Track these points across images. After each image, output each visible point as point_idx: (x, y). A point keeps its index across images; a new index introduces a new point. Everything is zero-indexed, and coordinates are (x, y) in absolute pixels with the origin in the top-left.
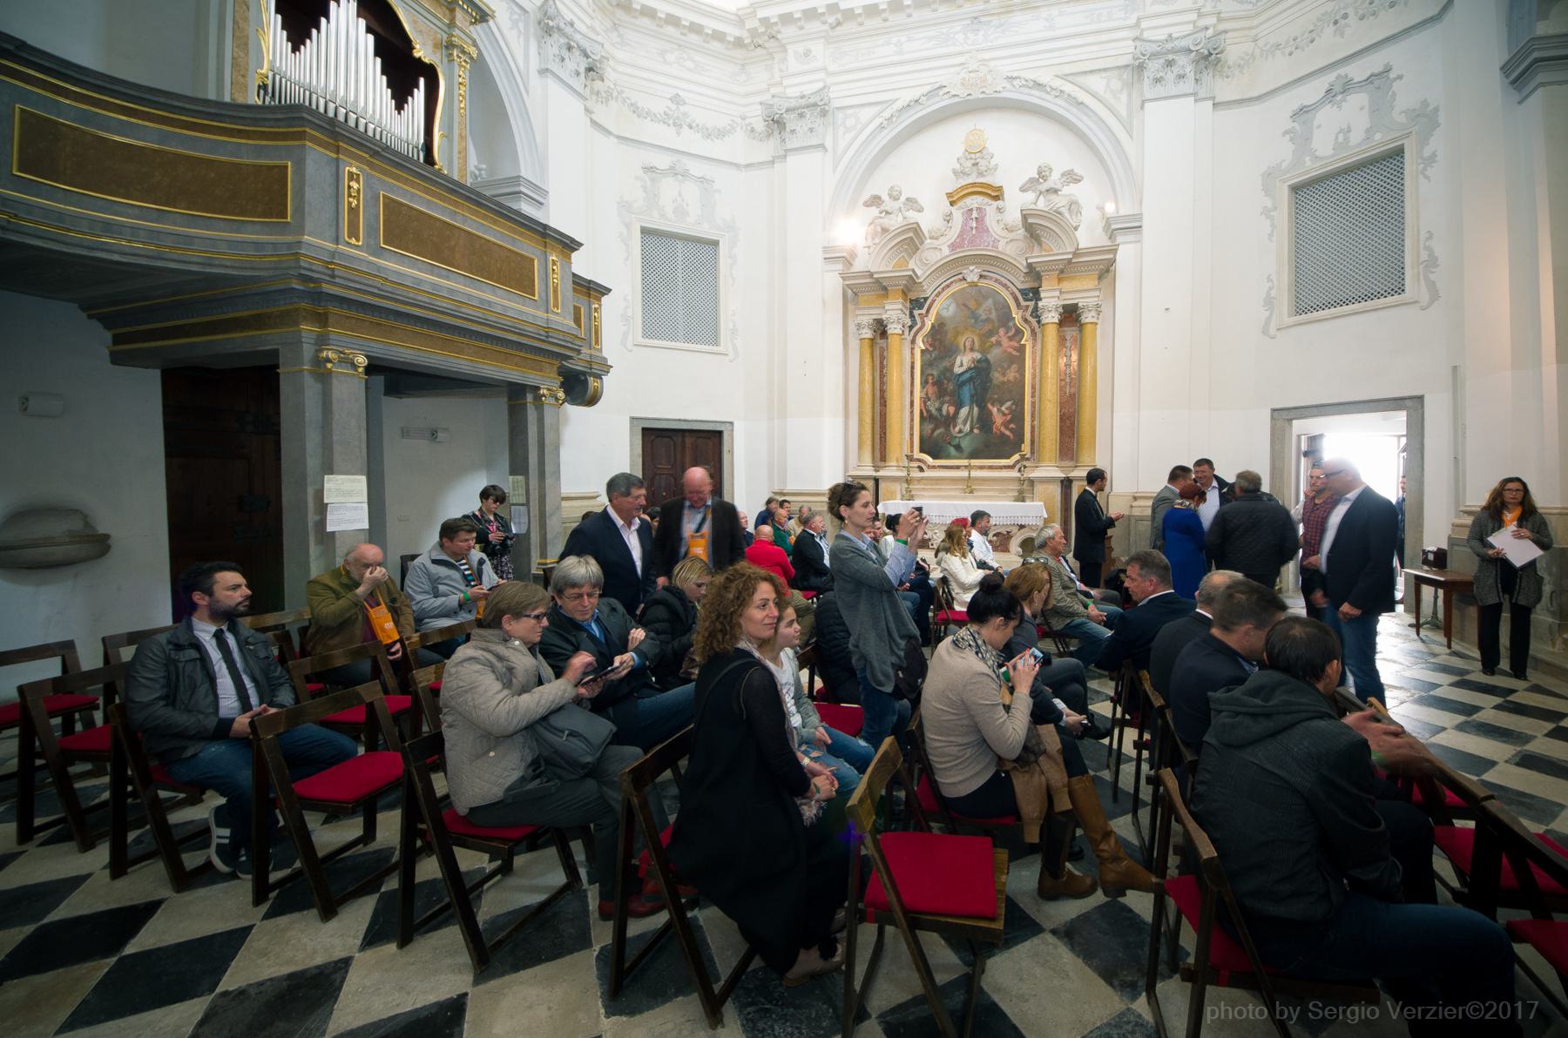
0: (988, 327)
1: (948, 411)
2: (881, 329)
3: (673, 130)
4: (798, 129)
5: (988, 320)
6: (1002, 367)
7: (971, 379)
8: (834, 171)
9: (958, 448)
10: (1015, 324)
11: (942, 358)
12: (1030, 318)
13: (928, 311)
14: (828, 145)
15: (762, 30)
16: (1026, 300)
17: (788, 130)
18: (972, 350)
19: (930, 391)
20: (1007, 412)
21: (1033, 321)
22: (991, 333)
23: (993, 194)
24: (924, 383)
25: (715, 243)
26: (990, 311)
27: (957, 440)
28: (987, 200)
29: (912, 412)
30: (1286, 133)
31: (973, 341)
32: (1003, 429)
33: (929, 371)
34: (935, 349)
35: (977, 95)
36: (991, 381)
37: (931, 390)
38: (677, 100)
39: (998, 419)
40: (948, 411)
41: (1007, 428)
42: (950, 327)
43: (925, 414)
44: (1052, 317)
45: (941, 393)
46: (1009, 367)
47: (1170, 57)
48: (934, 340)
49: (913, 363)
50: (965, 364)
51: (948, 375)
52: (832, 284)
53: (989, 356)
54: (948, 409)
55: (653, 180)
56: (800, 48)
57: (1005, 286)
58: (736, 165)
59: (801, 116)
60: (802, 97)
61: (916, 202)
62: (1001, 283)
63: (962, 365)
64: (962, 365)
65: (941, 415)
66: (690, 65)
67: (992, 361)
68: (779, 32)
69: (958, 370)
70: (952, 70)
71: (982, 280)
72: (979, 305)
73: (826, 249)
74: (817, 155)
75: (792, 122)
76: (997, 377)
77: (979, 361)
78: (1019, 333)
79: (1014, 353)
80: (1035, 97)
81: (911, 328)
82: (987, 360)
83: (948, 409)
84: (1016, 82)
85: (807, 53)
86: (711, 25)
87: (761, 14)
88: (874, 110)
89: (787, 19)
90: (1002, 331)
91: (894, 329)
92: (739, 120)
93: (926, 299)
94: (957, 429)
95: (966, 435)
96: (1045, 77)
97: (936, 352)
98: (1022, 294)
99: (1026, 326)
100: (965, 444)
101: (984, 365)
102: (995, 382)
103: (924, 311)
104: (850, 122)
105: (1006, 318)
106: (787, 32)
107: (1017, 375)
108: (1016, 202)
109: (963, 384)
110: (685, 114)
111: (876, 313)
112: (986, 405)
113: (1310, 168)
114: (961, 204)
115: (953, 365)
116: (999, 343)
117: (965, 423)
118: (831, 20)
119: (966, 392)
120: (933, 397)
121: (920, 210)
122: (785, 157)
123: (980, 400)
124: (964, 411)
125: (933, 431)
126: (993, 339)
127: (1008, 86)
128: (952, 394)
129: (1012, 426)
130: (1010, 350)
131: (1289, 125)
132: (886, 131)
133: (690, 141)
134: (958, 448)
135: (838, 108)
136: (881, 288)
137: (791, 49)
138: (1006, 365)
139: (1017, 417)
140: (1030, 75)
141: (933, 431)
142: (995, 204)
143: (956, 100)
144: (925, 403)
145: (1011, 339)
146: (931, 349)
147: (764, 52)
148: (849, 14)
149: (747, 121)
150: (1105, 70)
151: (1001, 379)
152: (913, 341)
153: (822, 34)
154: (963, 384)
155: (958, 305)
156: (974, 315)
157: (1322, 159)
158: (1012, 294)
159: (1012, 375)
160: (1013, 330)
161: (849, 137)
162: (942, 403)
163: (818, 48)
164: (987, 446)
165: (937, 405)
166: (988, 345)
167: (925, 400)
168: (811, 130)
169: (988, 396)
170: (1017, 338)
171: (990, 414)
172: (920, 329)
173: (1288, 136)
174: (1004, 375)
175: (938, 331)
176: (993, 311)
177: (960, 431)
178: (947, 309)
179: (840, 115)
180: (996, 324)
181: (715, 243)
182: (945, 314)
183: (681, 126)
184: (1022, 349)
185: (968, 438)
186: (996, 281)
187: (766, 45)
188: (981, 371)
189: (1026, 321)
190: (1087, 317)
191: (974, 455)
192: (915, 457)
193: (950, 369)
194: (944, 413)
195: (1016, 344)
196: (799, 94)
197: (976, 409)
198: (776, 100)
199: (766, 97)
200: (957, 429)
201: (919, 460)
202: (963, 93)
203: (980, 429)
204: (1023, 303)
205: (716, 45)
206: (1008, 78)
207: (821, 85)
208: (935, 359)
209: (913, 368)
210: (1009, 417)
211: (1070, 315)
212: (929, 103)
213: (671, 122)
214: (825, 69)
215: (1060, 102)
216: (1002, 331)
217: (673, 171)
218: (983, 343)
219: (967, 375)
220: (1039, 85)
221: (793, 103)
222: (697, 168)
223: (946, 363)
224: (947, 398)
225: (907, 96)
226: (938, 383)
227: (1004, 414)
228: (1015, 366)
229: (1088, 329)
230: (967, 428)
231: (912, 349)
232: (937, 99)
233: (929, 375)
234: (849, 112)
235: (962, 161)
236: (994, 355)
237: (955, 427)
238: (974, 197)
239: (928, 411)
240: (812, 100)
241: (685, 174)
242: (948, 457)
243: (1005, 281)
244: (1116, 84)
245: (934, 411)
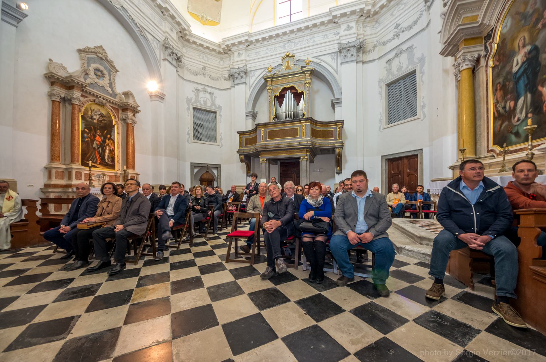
9: (517, 134)
11: (504, 67)
27: (516, 128)
31: (525, 39)
37: (499, 94)
40: (510, 107)
48: (499, 55)
49: (487, 81)
51: (509, 77)
63: (518, 63)
65: (506, 111)
67: (539, 46)
69: (515, 69)
77: (530, 52)
93: (492, 30)
94: (516, 119)
97: (501, 64)
112: (537, 89)
119: (522, 84)
120: (500, 100)
124: (521, 101)
125: (501, 126)
134: (517, 134)
141: (501, 126)
144: (496, 106)
146: (498, 64)
152: (487, 66)
154: (519, 78)
162: (506, 102)
165: (503, 104)
167: (495, 105)
172: (490, 54)
177: (519, 120)
192: (490, 149)
193: (510, 72)
194: (507, 109)
197: (529, 96)
200: (516, 119)
201: (492, 151)
208: (501, 69)
209: (487, 84)
219: (522, 69)
223: (507, 69)
224: (509, 96)
226: (504, 88)
231: (486, 71)
233: (498, 84)
239: (498, 112)
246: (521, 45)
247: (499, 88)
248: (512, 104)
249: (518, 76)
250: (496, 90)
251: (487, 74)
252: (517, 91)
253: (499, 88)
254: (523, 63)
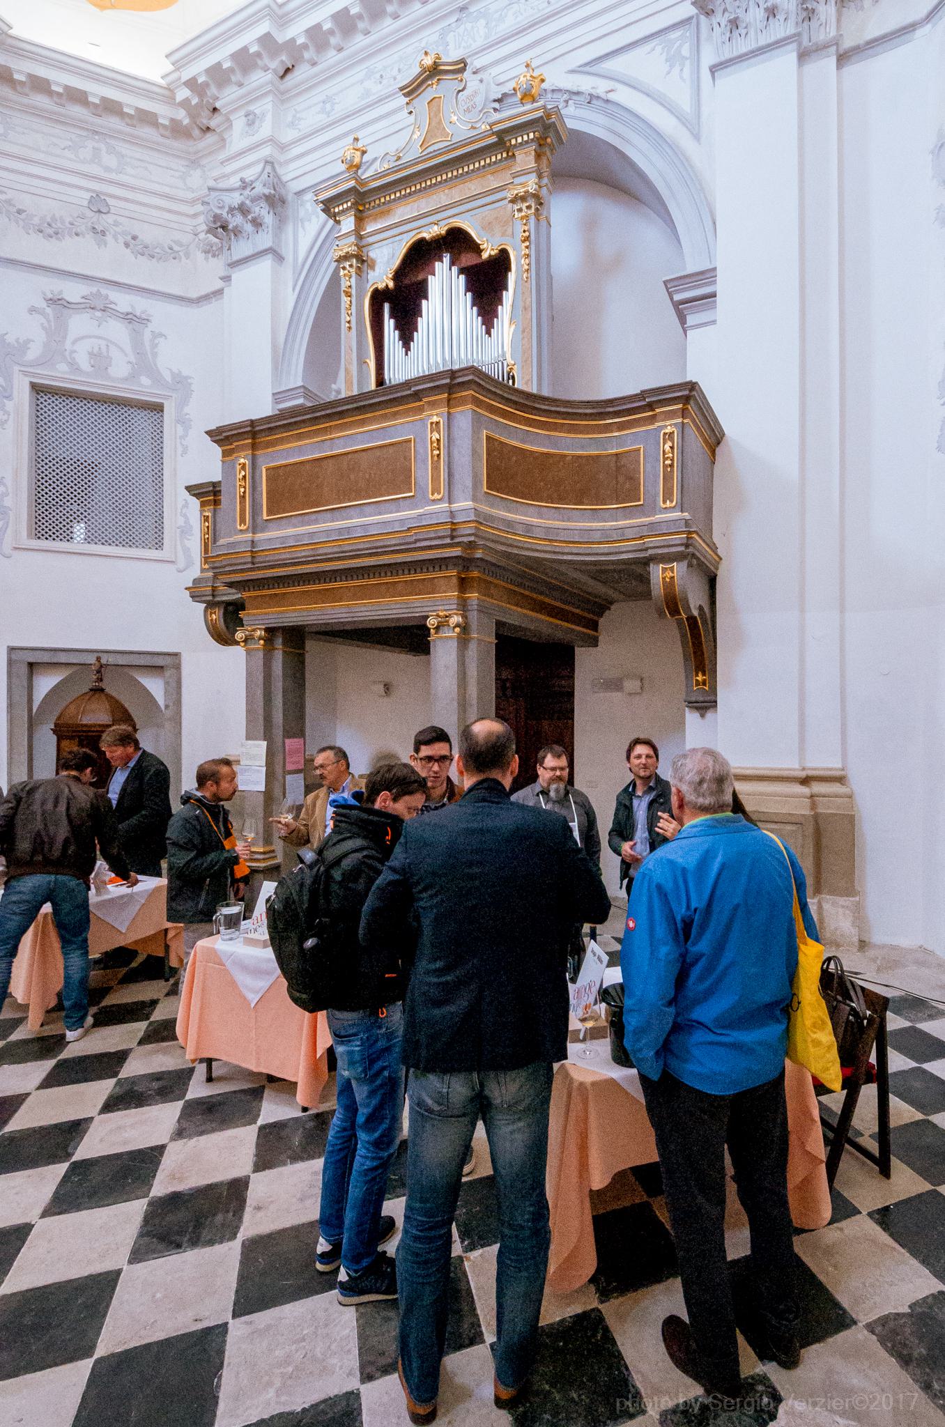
15: (195, 101)
25: (158, 408)
66: (111, 161)
74: (267, 263)
86: (131, 102)
89: (219, 75)
106: (227, 97)
118: (276, 64)
135: (299, 193)
153: (269, 88)
181: (158, 408)
187: (212, 124)
198: (214, 194)
205: (147, 132)
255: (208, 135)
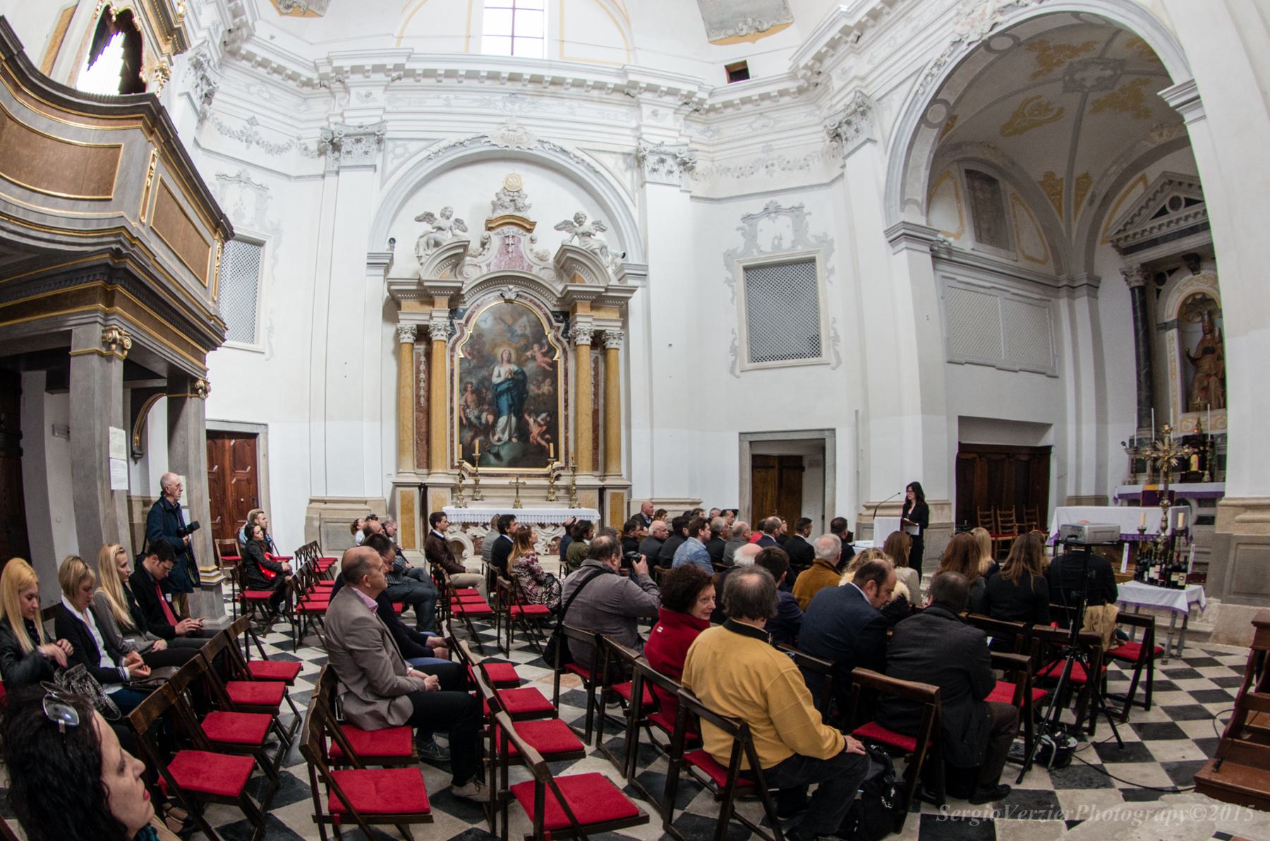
0: (522, 342)
1: (487, 421)
2: (423, 334)
3: (244, 143)
4: (354, 151)
5: (523, 336)
6: (538, 381)
7: (508, 390)
8: (381, 188)
9: (497, 456)
10: (548, 342)
11: (481, 367)
12: (561, 338)
13: (467, 321)
14: (379, 168)
16: (558, 321)
17: (343, 150)
18: (509, 361)
19: (469, 399)
20: (542, 423)
21: (564, 341)
22: (527, 347)
23: (528, 227)
24: (463, 391)
26: (525, 327)
28: (521, 231)
29: (452, 419)
30: (738, 229)
31: (510, 354)
32: (539, 439)
33: (468, 379)
34: (473, 358)
35: (513, 147)
36: (527, 393)
37: (470, 397)
38: (252, 121)
39: (535, 430)
40: (487, 421)
41: (543, 438)
42: (487, 339)
43: (464, 421)
44: (585, 340)
45: (480, 401)
46: (543, 381)
47: (664, 157)
49: (452, 370)
50: (502, 374)
51: (487, 383)
52: (375, 290)
53: (525, 369)
54: (487, 417)
55: (222, 186)
56: (363, 91)
57: (538, 306)
58: (288, 176)
59: (358, 141)
60: (361, 127)
61: (463, 223)
62: (535, 304)
63: (499, 376)
64: (499, 376)
65: (480, 423)
67: (527, 374)
68: (348, 78)
69: (496, 380)
70: (495, 126)
71: (518, 299)
72: (515, 320)
73: (370, 255)
74: (370, 173)
75: (347, 145)
76: (532, 389)
77: (516, 373)
78: (551, 350)
79: (548, 368)
80: (560, 159)
81: (450, 335)
82: (523, 373)
83: (487, 417)
84: (545, 145)
85: (368, 95)
87: (336, 64)
88: (423, 144)
90: (536, 347)
91: (437, 336)
92: (295, 140)
94: (496, 438)
95: (505, 443)
96: (569, 147)
97: (475, 361)
98: (554, 316)
99: (558, 345)
100: (504, 452)
101: (520, 377)
102: (531, 394)
103: (463, 321)
104: (399, 151)
105: (539, 336)
107: (551, 389)
108: (549, 242)
109: (501, 393)
110: (256, 133)
111: (422, 319)
112: (523, 416)
113: (756, 258)
114: (499, 230)
115: (491, 375)
116: (533, 358)
117: (503, 431)
118: (395, 75)
119: (504, 402)
121: (465, 230)
122: (338, 173)
123: (518, 409)
124: (503, 420)
126: (529, 354)
127: (539, 147)
128: (490, 404)
129: (547, 436)
130: (543, 365)
131: (741, 224)
132: (431, 162)
133: (256, 154)
134: (497, 456)
135: (389, 139)
136: (426, 295)
137: (353, 91)
138: (540, 379)
139: (551, 429)
140: (559, 143)
142: (529, 235)
143: (495, 148)
144: (464, 410)
145: (544, 355)
147: (327, 90)
148: (411, 74)
149: (302, 141)
150: (614, 153)
151: (537, 391)
152: (453, 349)
154: (501, 393)
155: (495, 319)
156: (510, 329)
157: (765, 253)
158: (545, 314)
159: (546, 388)
160: (546, 347)
161: (397, 162)
162: (481, 412)
163: (378, 93)
164: (524, 455)
165: (476, 413)
166: (524, 358)
167: (465, 407)
168: (366, 153)
169: (525, 406)
170: (551, 354)
171: (527, 423)
173: (740, 232)
174: (539, 388)
175: (477, 339)
176: (528, 328)
177: (499, 440)
178: (485, 321)
179: (390, 145)
180: (531, 340)
182: (484, 326)
183: (251, 142)
184: (554, 365)
185: (507, 447)
186: (531, 301)
187: (332, 86)
188: (518, 383)
189: (558, 340)
190: (611, 344)
191: (513, 463)
194: (483, 421)
195: (549, 361)
196: (357, 124)
197: (514, 419)
199: (325, 124)
200: (496, 438)
202: (502, 144)
203: (519, 438)
204: (555, 324)
206: (539, 141)
207: (377, 120)
208: (474, 367)
209: (452, 375)
210: (544, 428)
211: (598, 340)
212: (472, 146)
213: (244, 138)
214: (384, 109)
215: (579, 166)
216: (536, 347)
217: (239, 179)
218: (519, 356)
219: (505, 386)
220: (564, 151)
221: (352, 131)
222: (257, 177)
223: (484, 373)
224: (486, 407)
225: (453, 139)
226: (477, 392)
227: (540, 425)
228: (548, 380)
229: (612, 354)
230: (506, 437)
232: (478, 145)
233: (468, 383)
234: (399, 143)
235: (502, 196)
236: (530, 368)
237: (494, 435)
238: (511, 227)
239: (468, 419)
240: (370, 130)
241: (247, 182)
242: (488, 465)
243: (539, 302)
244: (621, 164)
245: (473, 419)
246: (505, 358)
247: (469, 389)
248: (491, 418)
249: (499, 389)
250: (465, 390)
251: (452, 361)
252: (498, 407)
253: (469, 389)
254: (507, 380)
255: (323, 88)
